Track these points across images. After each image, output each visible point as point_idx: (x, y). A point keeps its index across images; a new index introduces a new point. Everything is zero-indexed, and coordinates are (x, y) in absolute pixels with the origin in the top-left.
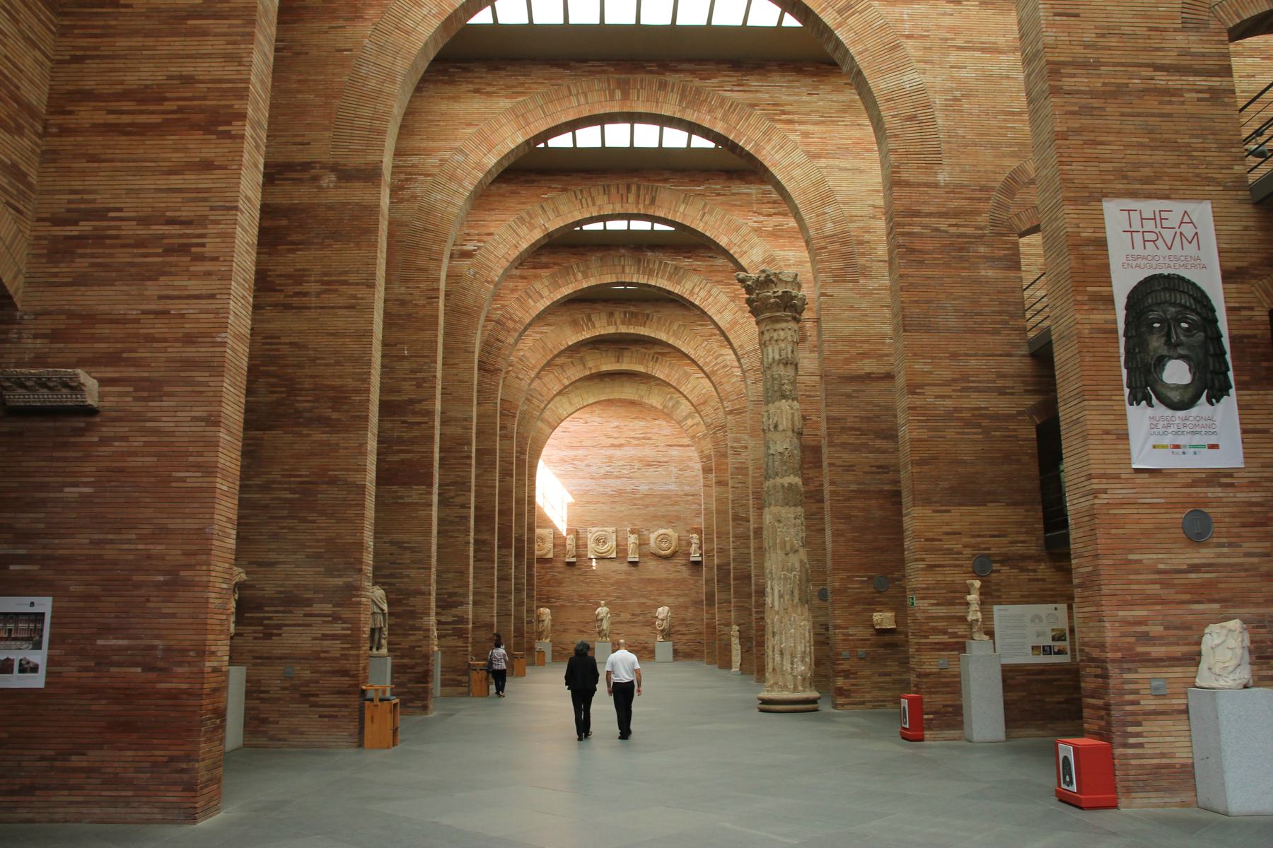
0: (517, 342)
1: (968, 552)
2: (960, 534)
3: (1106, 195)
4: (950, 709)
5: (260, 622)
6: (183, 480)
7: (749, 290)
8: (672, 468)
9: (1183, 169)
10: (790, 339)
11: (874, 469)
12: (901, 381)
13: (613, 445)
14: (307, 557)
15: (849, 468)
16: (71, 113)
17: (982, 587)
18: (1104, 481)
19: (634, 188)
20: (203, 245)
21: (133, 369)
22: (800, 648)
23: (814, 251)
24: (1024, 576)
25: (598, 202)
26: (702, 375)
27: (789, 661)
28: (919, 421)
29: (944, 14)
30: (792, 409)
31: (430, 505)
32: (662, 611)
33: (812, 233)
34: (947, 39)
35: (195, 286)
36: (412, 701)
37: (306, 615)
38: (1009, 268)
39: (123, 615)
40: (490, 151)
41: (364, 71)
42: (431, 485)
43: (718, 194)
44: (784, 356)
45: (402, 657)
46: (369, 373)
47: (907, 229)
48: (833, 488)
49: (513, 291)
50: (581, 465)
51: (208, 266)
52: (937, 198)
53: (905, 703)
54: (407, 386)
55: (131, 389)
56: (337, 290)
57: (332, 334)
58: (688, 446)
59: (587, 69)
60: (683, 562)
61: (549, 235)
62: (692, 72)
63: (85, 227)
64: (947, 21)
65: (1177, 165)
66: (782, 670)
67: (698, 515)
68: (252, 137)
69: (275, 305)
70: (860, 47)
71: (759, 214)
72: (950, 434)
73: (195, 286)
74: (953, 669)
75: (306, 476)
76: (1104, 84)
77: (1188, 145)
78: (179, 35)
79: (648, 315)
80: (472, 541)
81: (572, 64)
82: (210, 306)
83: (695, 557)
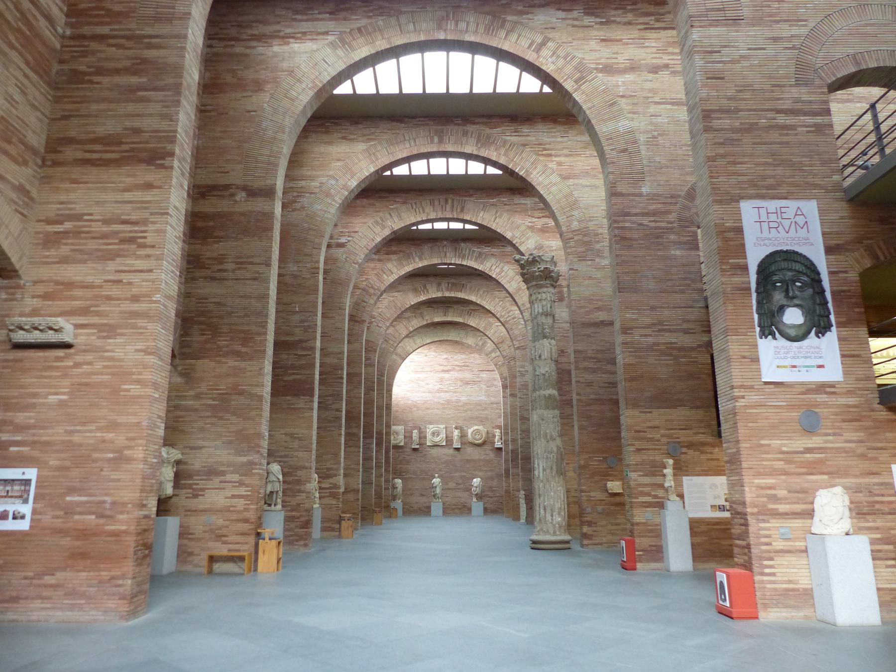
0: (376, 303)
1: (664, 440)
2: (658, 427)
3: (742, 198)
4: (654, 548)
5: (190, 487)
6: (128, 390)
7: (522, 267)
8: (482, 386)
9: (797, 179)
10: (549, 299)
11: (606, 385)
12: (617, 325)
13: (443, 371)
14: (223, 443)
15: (589, 384)
16: (59, 152)
17: (674, 464)
18: (743, 390)
19: (450, 201)
20: (145, 238)
21: (97, 318)
22: (558, 505)
23: (565, 241)
24: (704, 457)
25: (427, 211)
26: (500, 324)
27: (550, 514)
28: (630, 352)
29: (646, 81)
30: (551, 345)
31: (312, 409)
32: (476, 481)
33: (564, 229)
34: (648, 97)
35: (139, 264)
36: (297, 541)
37: (221, 482)
38: (691, 249)
39: (85, 480)
40: (352, 177)
41: (264, 125)
42: (313, 396)
43: (506, 205)
44: (545, 310)
45: (292, 511)
46: (267, 322)
47: (621, 225)
48: (578, 397)
49: (373, 269)
50: (423, 384)
51: (148, 251)
52: (640, 203)
53: (623, 543)
54: (298, 331)
55: (95, 331)
56: (246, 268)
57: (242, 297)
59: (415, 123)
61: (395, 232)
62: (485, 124)
63: (68, 225)
64: (648, 85)
65: (792, 176)
66: (545, 521)
67: (500, 417)
68: (179, 167)
69: (205, 278)
70: (589, 105)
71: (533, 217)
72: (651, 360)
73: (139, 264)
74: (657, 520)
75: (223, 389)
76: (741, 124)
77: (801, 162)
78: (132, 101)
79: (463, 284)
80: (343, 433)
81: (406, 120)
82: (149, 277)
83: (498, 444)
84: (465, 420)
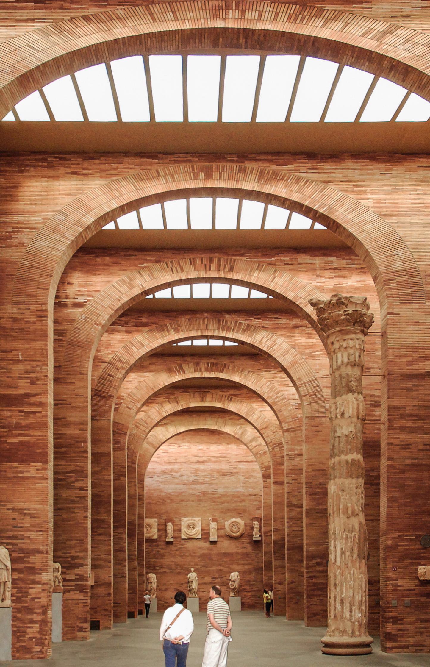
13: (198, 462)
58: (252, 462)
60: (248, 541)
67: (259, 508)
84: (222, 512)
